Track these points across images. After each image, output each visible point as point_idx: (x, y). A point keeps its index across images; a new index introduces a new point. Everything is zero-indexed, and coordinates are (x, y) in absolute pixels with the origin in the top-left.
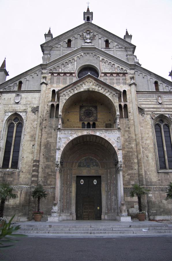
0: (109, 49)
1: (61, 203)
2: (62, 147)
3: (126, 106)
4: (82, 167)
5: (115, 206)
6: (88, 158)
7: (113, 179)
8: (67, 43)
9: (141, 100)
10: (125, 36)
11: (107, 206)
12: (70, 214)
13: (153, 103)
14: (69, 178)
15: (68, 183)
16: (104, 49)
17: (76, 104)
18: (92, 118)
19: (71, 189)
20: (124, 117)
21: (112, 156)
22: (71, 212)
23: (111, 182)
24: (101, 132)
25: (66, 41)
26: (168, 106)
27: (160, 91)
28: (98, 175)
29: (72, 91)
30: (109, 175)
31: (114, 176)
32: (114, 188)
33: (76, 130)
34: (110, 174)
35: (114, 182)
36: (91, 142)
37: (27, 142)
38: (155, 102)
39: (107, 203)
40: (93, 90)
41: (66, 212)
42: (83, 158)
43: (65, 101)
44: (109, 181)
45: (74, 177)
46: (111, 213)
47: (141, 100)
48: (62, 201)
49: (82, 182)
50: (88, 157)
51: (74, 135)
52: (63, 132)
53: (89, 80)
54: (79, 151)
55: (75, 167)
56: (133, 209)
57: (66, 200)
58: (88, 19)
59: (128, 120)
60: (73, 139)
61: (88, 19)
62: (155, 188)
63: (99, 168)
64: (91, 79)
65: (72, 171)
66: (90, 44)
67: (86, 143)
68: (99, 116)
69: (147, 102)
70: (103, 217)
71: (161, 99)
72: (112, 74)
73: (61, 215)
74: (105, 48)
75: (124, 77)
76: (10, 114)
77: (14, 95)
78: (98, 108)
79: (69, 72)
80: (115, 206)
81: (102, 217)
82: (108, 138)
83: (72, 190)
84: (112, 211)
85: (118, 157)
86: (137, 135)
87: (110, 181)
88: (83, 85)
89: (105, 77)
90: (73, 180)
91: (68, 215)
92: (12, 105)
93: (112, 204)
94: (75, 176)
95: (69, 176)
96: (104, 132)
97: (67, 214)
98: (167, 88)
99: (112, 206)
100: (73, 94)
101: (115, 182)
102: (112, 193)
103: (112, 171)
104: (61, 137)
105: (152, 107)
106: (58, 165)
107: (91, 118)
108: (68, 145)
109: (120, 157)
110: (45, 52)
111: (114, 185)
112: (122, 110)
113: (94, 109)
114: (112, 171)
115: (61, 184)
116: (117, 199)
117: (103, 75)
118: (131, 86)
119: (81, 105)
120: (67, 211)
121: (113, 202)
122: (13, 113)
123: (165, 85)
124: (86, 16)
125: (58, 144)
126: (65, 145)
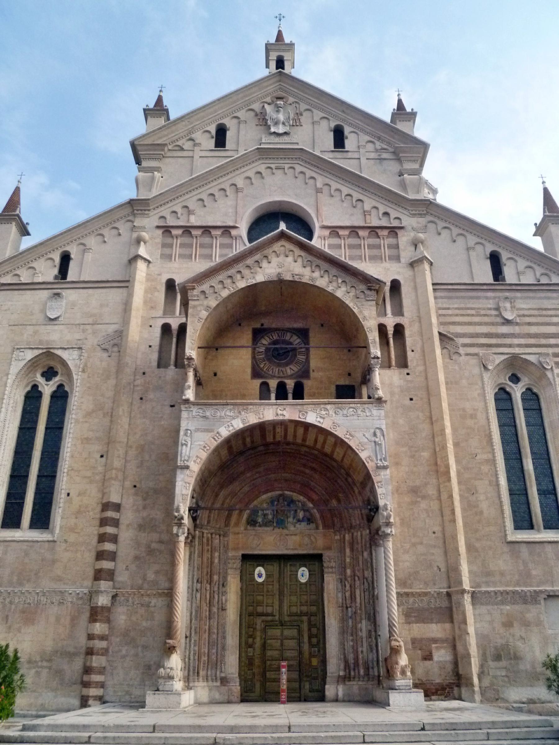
0: (345, 155)
1: (192, 646)
3: (399, 330)
4: (260, 526)
5: (370, 657)
6: (281, 495)
8: (213, 137)
9: (450, 312)
10: (393, 115)
11: (344, 654)
12: (221, 683)
13: (486, 319)
14: (216, 561)
15: (216, 577)
16: (331, 155)
17: (240, 325)
18: (291, 366)
19: (224, 598)
20: (393, 363)
21: (356, 491)
22: (223, 675)
23: (354, 575)
24: (323, 412)
25: (213, 129)
26: (534, 330)
27: (508, 282)
28: (311, 552)
29: (229, 281)
30: (348, 551)
31: (366, 554)
34: (352, 550)
35: (366, 575)
36: (288, 444)
37: (82, 443)
38: (491, 316)
39: (342, 644)
40: (297, 279)
42: (264, 497)
43: (204, 314)
44: (349, 572)
45: (234, 558)
47: (450, 312)
49: (260, 576)
50: (280, 492)
52: (195, 410)
53: (282, 248)
54: (248, 475)
55: (237, 524)
56: (427, 663)
58: (280, 63)
59: (408, 374)
61: (280, 63)
62: (502, 593)
63: (317, 528)
64: (289, 246)
65: (226, 539)
66: (286, 139)
67: (272, 447)
68: (313, 363)
69: (468, 315)
70: (330, 690)
71: (511, 307)
72: (354, 230)
73: (191, 685)
74: (333, 151)
75: (392, 241)
76: (30, 355)
77: (44, 294)
78: (311, 334)
79: (219, 224)
81: (327, 693)
83: (226, 601)
84: (359, 673)
85: (379, 491)
86: (437, 421)
87: (353, 571)
88: (264, 264)
89: (335, 241)
90: (231, 568)
91: (215, 684)
92: (37, 328)
93: (360, 649)
94: (237, 554)
95: (217, 554)
97: (210, 683)
98: (529, 272)
99: (360, 656)
100: (233, 291)
101: (367, 574)
103: (359, 538)
104: (193, 428)
105: (482, 334)
106: (182, 518)
107: (288, 369)
108: (216, 454)
109: (384, 492)
110: (144, 164)
111: (366, 584)
112: (388, 343)
113: (298, 340)
115: (193, 583)
116: (376, 631)
117: (327, 232)
118: (416, 269)
119: (258, 326)
120: (209, 673)
121: (362, 642)
122: (41, 351)
123: (522, 264)
124: (274, 56)
125: (184, 451)
126: (204, 455)
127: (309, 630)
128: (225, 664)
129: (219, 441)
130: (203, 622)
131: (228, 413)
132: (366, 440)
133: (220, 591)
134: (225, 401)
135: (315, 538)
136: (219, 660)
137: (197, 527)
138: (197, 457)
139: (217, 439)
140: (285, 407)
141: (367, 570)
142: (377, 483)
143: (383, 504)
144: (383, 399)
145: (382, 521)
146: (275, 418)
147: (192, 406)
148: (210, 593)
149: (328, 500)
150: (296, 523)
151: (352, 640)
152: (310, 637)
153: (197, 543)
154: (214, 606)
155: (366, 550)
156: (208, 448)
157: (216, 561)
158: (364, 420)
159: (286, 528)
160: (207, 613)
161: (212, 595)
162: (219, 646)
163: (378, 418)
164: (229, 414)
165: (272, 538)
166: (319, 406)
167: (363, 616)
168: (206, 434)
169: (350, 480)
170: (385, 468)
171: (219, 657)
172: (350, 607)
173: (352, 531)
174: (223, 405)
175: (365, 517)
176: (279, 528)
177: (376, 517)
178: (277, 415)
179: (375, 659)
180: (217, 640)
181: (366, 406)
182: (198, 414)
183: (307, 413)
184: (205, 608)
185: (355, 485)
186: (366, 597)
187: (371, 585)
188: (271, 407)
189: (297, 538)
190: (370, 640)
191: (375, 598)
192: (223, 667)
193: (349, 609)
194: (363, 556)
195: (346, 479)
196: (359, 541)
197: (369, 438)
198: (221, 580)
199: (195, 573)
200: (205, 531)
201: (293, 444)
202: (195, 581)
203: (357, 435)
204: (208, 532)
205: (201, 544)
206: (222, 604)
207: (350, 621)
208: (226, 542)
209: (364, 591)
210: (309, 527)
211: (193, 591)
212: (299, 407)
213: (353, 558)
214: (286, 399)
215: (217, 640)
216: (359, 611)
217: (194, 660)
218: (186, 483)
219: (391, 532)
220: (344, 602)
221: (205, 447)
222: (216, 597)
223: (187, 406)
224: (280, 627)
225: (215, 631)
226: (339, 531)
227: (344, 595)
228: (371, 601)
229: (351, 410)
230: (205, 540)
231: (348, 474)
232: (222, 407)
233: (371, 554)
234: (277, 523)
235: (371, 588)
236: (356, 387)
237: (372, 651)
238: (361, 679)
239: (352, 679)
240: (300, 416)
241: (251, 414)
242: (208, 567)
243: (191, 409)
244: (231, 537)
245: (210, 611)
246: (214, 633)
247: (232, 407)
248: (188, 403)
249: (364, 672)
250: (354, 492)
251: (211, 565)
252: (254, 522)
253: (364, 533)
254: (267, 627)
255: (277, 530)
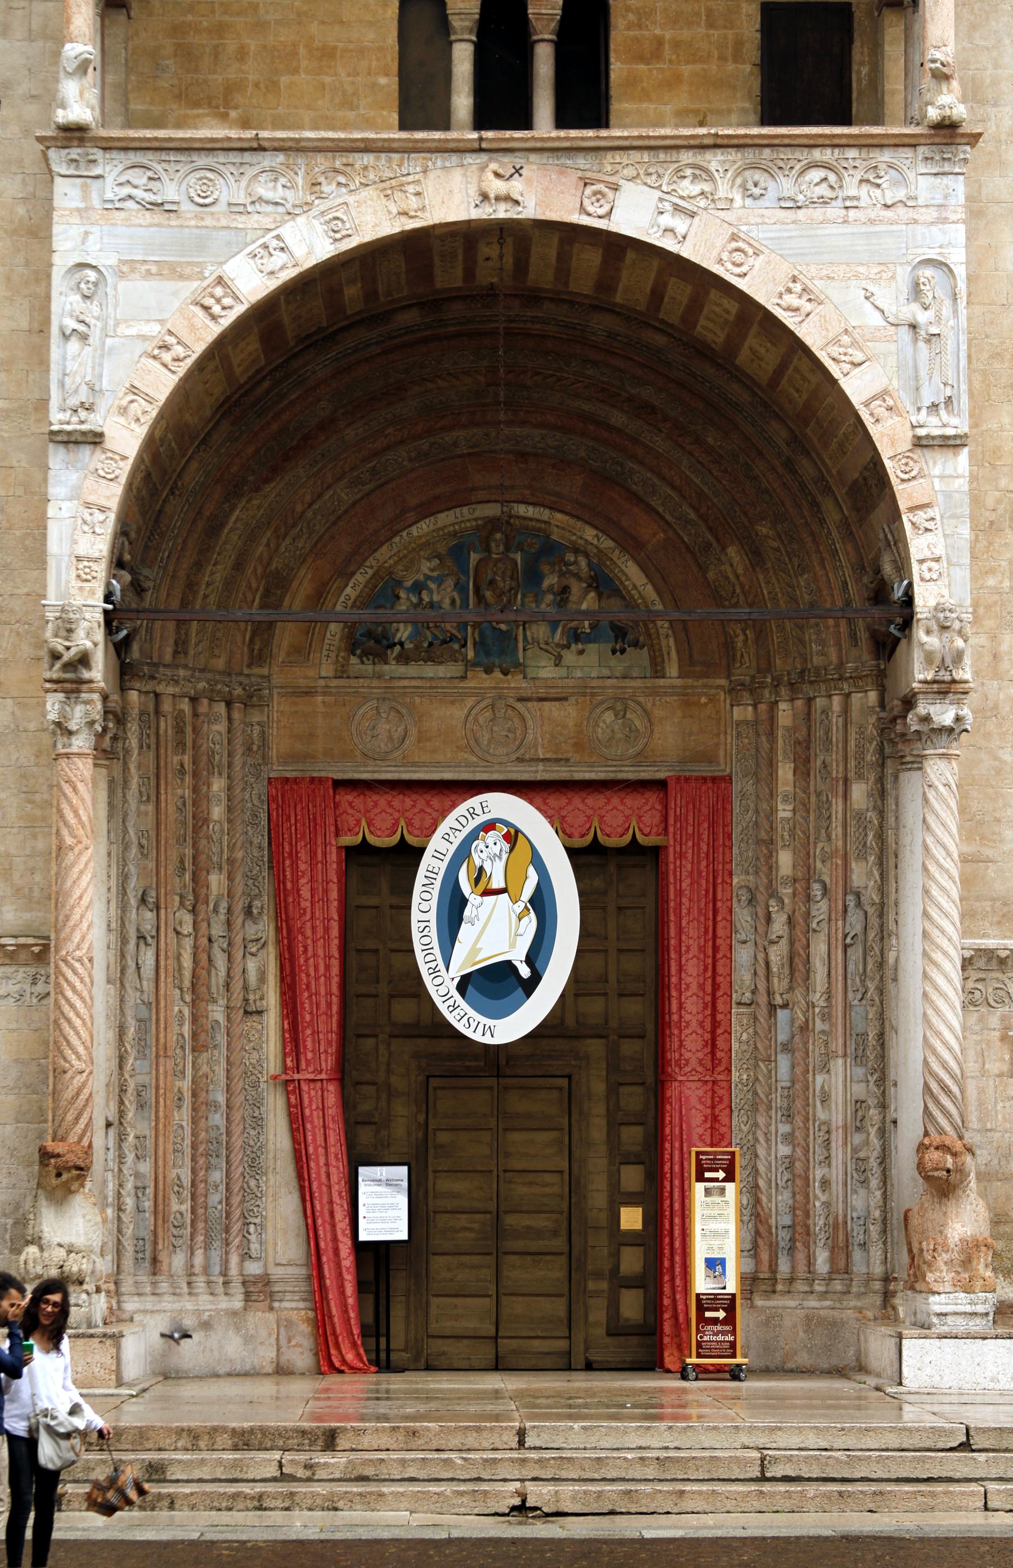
1: (130, 1158)
2: (123, 411)
5: (858, 1201)
6: (493, 524)
7: (837, 831)
12: (248, 1296)
15: (216, 881)
21: (832, 516)
22: (254, 1268)
24: (688, 187)
30: (785, 772)
31: (859, 793)
32: (856, 954)
33: (322, 162)
34: (803, 768)
36: (533, 297)
41: (190, 1273)
42: (423, 528)
44: (785, 860)
46: (801, 1286)
48: (138, 1126)
50: (492, 510)
51: (290, 232)
55: (301, 653)
57: (183, 1116)
60: (273, 284)
65: (256, 717)
73: (131, 1305)
80: (858, 1201)
82: (785, 270)
84: (810, 1262)
85: (918, 546)
91: (224, 1303)
93: (818, 1173)
96: (723, 190)
99: (819, 1198)
102: (826, 1017)
103: (836, 721)
104: (106, 260)
106: (84, 660)
109: (940, 551)
111: (855, 919)
114: (836, 721)
115: (124, 907)
116: (883, 1106)
120: (199, 1260)
121: (827, 1143)
127: (613, 1089)
128: (262, 1227)
129: (228, 319)
130: (170, 1063)
131: (264, 190)
132: (876, 319)
133: (238, 940)
134: (249, 134)
135: (647, 714)
136: (237, 1213)
137: (135, 676)
138: (133, 389)
139: (216, 309)
140: (518, 160)
141: (862, 857)
142: (911, 509)
143: (932, 603)
144: (966, 128)
145: (920, 673)
146: (475, 214)
147: (98, 154)
148: (195, 947)
149: (707, 547)
150: (568, 647)
151: (789, 1139)
152: (615, 1123)
153: (134, 743)
154: (215, 1001)
155: (860, 777)
156: (179, 350)
157: (217, 812)
158: (872, 222)
159: (520, 667)
160: (186, 1029)
161: (204, 957)
162: (237, 1157)
163: (933, 214)
164: (269, 195)
165: (458, 713)
166: (674, 155)
167: (837, 1045)
168: (170, 286)
169: (806, 468)
170: (950, 444)
171: (236, 1200)
172: (785, 1006)
173: (809, 690)
174: (242, 150)
175: (863, 635)
176: (488, 671)
177: (903, 642)
178: (485, 197)
179: (877, 1214)
180: (229, 1133)
181: (886, 156)
182: (127, 190)
183: (616, 188)
184: (179, 1007)
185: (828, 490)
186: (851, 967)
187: (874, 921)
188: (455, 158)
189: (567, 714)
190: (858, 1139)
191: (889, 974)
192: (253, 1238)
193: (782, 1015)
194: (846, 796)
195: (789, 465)
196: (836, 735)
197: (890, 309)
198: (239, 889)
199: (132, 869)
200: (167, 689)
201: (557, 300)
202: (133, 902)
203: (833, 291)
204: (177, 690)
205: (153, 743)
206: (246, 988)
207: (784, 1063)
208: (257, 729)
209: (846, 947)
210: (618, 664)
211: (124, 941)
212: (581, 161)
213: (806, 806)
214: (527, 123)
215: (229, 1133)
216: (819, 1025)
217: (139, 1210)
218: (88, 505)
219: (958, 719)
220: (762, 985)
221: (165, 347)
222: (220, 961)
223: (75, 153)
224: (493, 1082)
225: (221, 1098)
226: (753, 689)
227: (761, 956)
228: (872, 986)
229: (816, 175)
230: (166, 726)
231: (798, 443)
232: (234, 157)
233: (882, 794)
234: (481, 645)
235: (871, 935)
236: (858, 15)
237: (865, 1182)
238: (819, 1288)
239: (779, 1287)
240: (587, 202)
241: (365, 193)
242: (181, 840)
243: (97, 171)
244: (279, 706)
245: (195, 1019)
246: (216, 1106)
247: (281, 158)
248: (82, 142)
249: (832, 1260)
250: (822, 521)
251: (196, 829)
252: (377, 641)
253: (856, 698)
254: (434, 1082)
255: (479, 680)
